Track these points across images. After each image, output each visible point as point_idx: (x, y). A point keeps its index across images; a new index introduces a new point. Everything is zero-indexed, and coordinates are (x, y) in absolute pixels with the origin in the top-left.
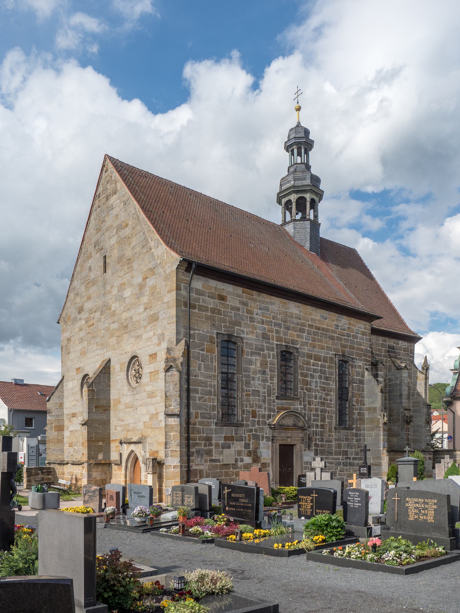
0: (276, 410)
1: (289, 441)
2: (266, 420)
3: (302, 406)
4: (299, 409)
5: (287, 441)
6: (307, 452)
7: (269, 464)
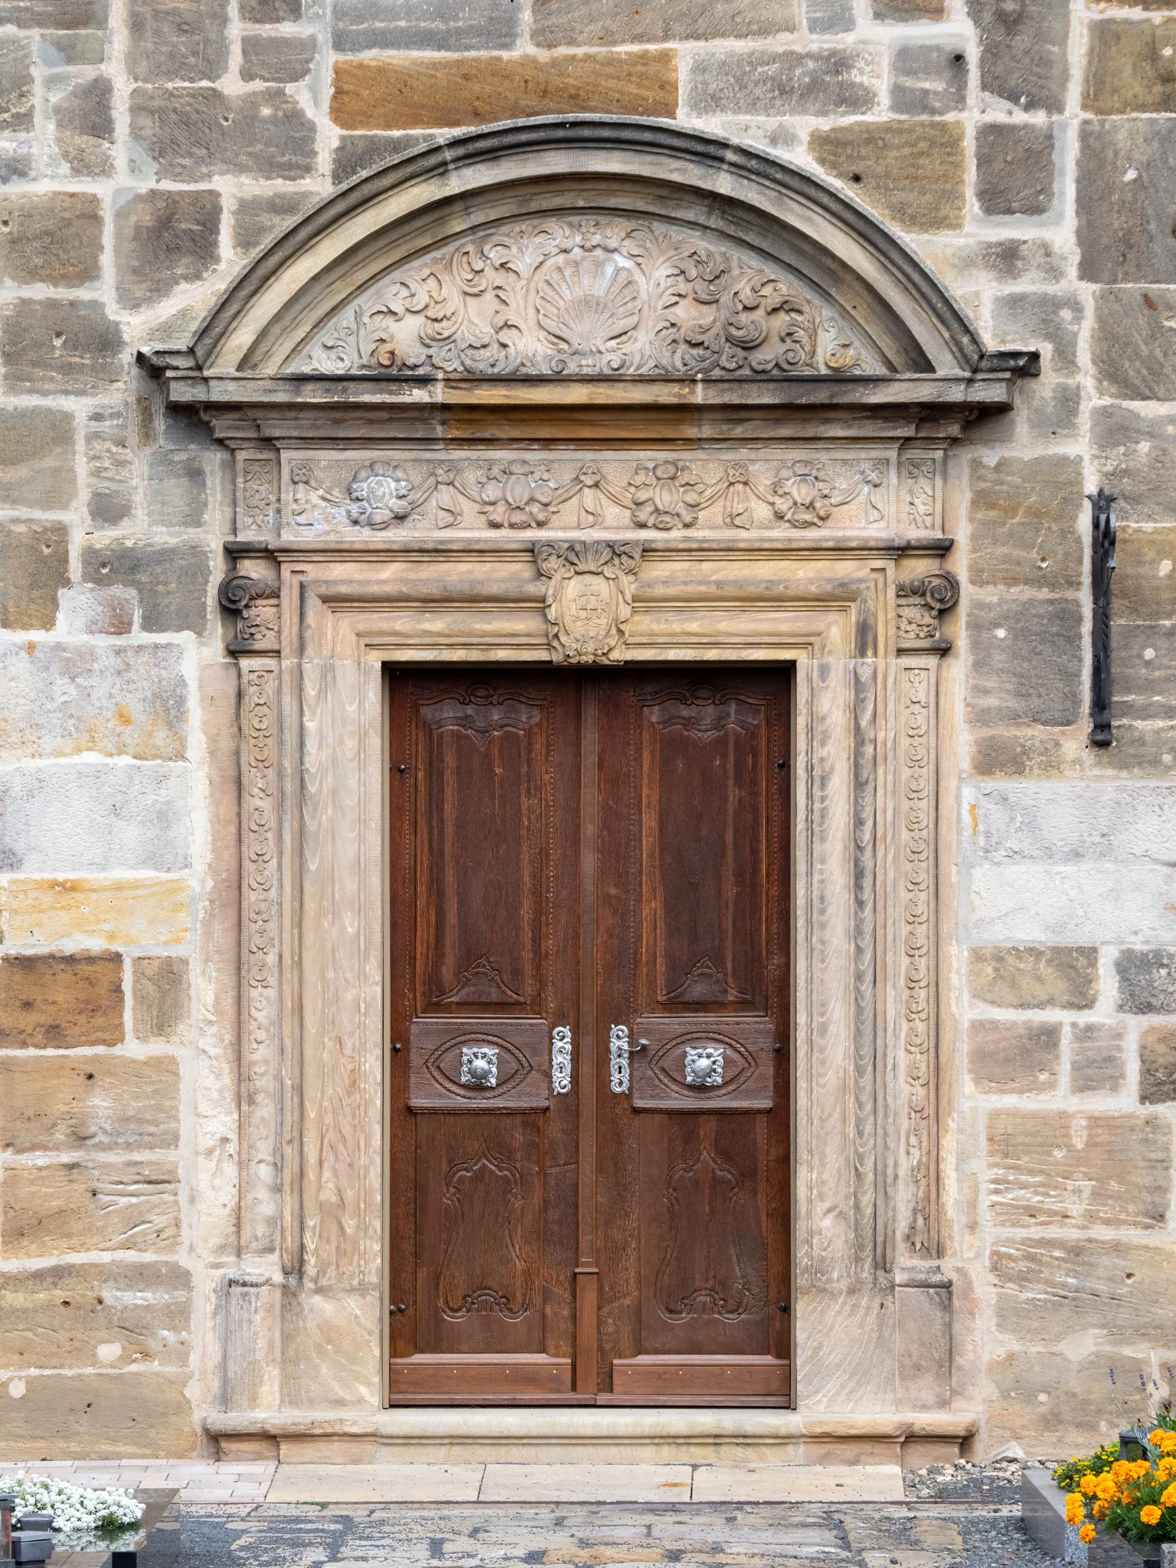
0: (329, 137)
1: (590, 620)
2: (104, 292)
3: (958, 29)
4: (878, 78)
5: (540, 604)
6: (1072, 790)
7: (168, 979)
